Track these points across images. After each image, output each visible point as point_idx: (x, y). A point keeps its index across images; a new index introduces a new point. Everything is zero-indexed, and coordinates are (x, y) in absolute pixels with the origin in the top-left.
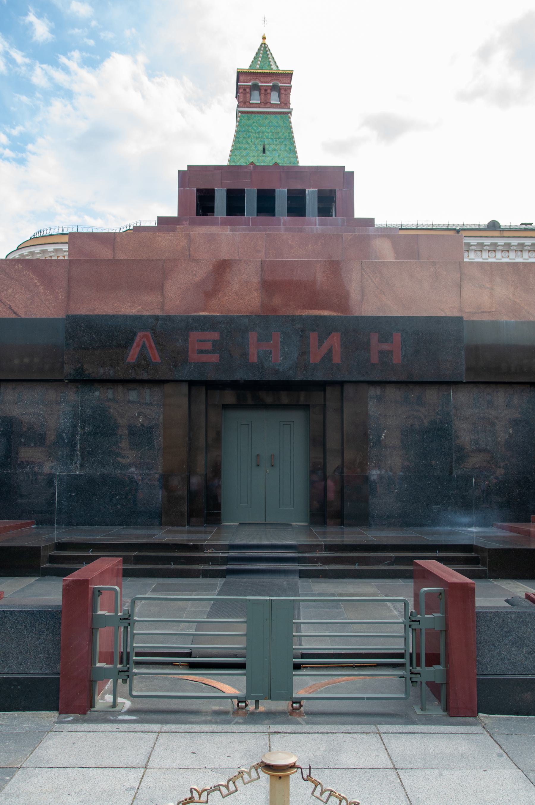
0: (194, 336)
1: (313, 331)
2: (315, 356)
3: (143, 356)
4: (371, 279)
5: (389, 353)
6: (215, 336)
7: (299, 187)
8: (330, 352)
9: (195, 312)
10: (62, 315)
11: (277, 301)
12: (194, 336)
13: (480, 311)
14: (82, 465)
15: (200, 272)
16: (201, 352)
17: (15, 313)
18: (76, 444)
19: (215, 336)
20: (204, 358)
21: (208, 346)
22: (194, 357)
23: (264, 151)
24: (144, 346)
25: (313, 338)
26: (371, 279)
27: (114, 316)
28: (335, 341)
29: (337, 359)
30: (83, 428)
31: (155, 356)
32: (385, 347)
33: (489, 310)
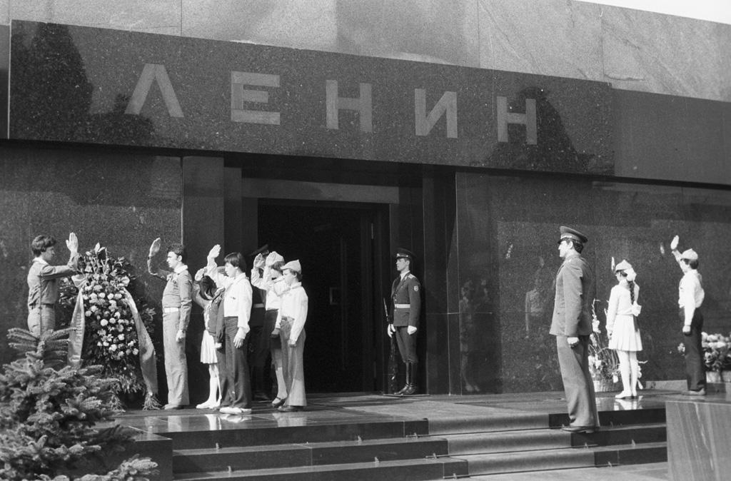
0: (237, 78)
1: (420, 87)
2: (423, 126)
4: (490, 15)
5: (522, 128)
6: (273, 80)
8: (443, 120)
9: (234, 38)
12: (237, 78)
13: (625, 77)
16: (251, 107)
19: (273, 80)
20: (257, 117)
21: (262, 97)
24: (155, 91)
25: (420, 95)
26: (490, 15)
27: (100, 30)
28: (449, 100)
29: (452, 132)
32: (517, 119)
33: (637, 78)
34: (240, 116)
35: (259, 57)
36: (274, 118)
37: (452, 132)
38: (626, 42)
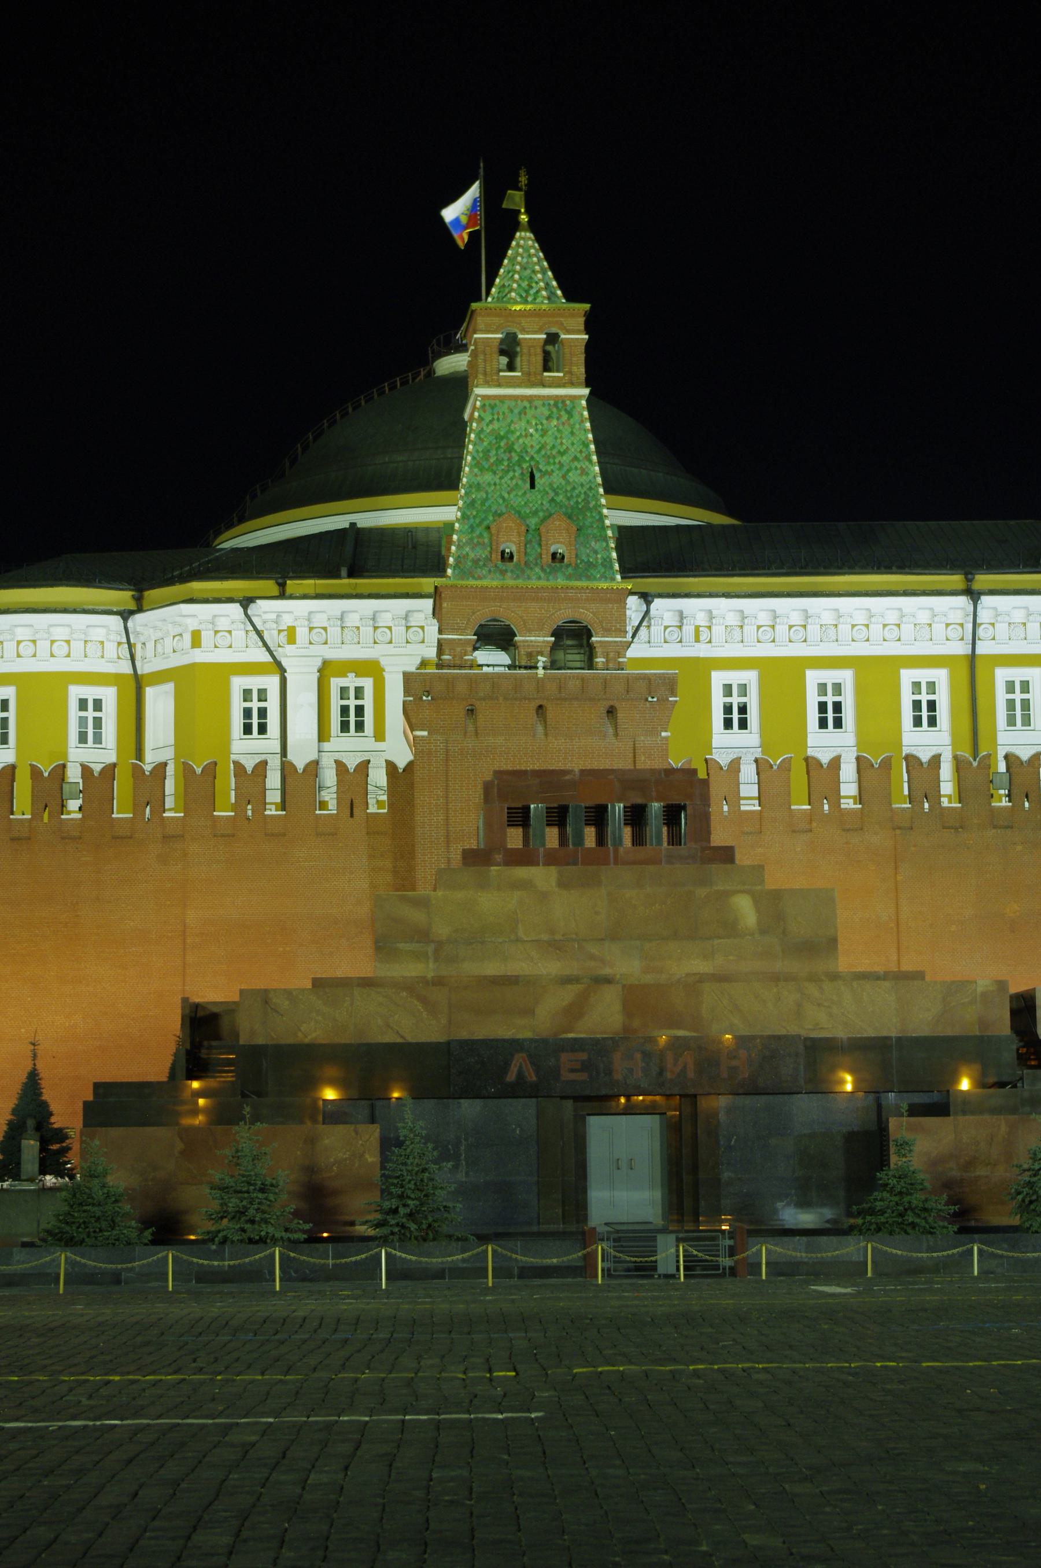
3: (520, 1075)
7: (639, 801)
8: (685, 1067)
10: (442, 1039)
11: (636, 1023)
12: (565, 1057)
14: (467, 1174)
15: (567, 995)
16: (573, 1071)
17: (402, 1037)
18: (461, 1155)
19: (584, 1056)
20: (573, 1076)
22: (566, 1076)
23: (533, 486)
24: (520, 1067)
29: (691, 1074)
30: (466, 1140)
31: (532, 1077)
34: (566, 1076)
35: (577, 1045)
36: (583, 1076)
37: (691, 1074)
38: (819, 1005)
